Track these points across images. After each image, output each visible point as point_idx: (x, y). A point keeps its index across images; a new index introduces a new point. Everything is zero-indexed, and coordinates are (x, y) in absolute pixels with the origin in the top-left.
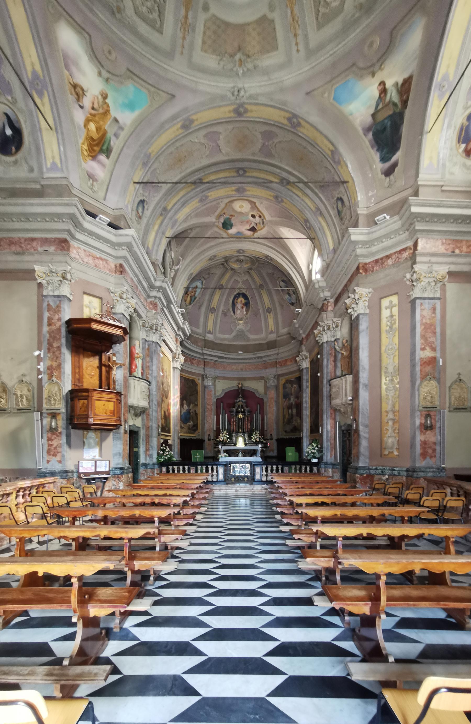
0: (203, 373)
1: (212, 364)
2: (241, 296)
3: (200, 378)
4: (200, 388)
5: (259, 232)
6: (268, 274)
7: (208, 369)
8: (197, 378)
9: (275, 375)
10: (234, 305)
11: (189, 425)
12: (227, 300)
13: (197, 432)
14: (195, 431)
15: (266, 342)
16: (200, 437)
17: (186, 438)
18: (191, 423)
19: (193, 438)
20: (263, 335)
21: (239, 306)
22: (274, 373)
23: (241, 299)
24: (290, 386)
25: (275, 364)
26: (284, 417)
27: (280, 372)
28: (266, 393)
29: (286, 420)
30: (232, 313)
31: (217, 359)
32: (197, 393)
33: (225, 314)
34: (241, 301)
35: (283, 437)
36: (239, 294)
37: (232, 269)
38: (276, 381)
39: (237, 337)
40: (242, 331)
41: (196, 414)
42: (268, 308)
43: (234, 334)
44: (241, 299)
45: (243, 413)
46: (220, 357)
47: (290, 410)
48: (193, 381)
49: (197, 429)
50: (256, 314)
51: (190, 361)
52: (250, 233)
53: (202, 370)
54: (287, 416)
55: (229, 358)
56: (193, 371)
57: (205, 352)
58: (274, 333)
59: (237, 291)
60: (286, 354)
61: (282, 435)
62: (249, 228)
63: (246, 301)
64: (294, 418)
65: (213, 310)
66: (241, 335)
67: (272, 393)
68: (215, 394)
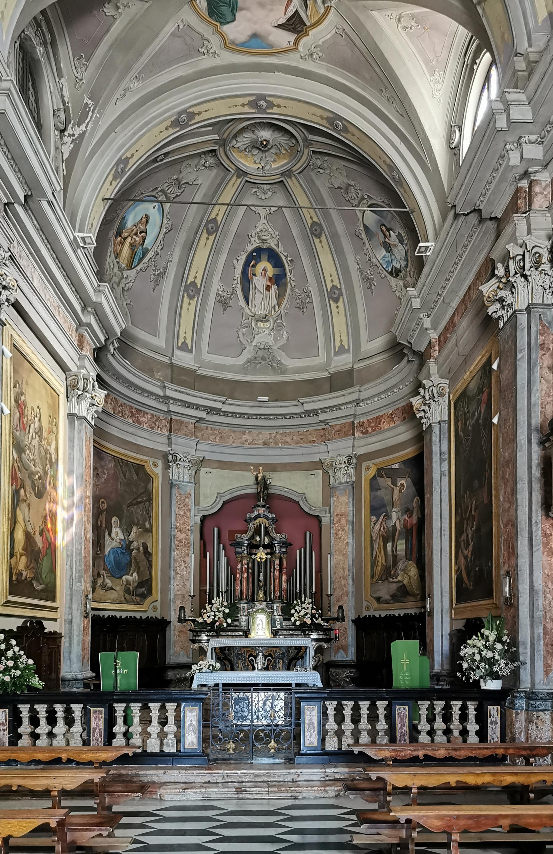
0: (165, 449)
1: (191, 427)
2: (264, 256)
3: (160, 463)
4: (158, 488)
5: (311, 33)
6: (334, 190)
7: (180, 440)
8: (151, 461)
9: (350, 457)
10: (246, 280)
11: (128, 583)
12: (229, 265)
13: (149, 600)
14: (144, 596)
15: (326, 374)
16: (158, 615)
17: (118, 615)
18: (133, 577)
19: (138, 615)
20: (321, 359)
21: (259, 282)
22: (349, 451)
23: (264, 264)
24: (389, 482)
25: (349, 429)
26: (373, 564)
27: (361, 451)
28: (326, 502)
29: (378, 569)
30: (242, 302)
31: (203, 414)
32: (150, 500)
33: (224, 303)
34: (265, 270)
35: (371, 613)
36: (258, 250)
37: (241, 173)
38: (352, 471)
39: (252, 364)
40: (267, 348)
41: (147, 554)
42: (334, 287)
43: (247, 355)
44: (264, 265)
45: (269, 546)
46: (211, 411)
47: (389, 545)
48: (140, 469)
49: (150, 592)
50: (303, 305)
51: (132, 415)
52: (285, 38)
53: (165, 440)
54: (381, 560)
55: (234, 415)
56: (140, 442)
57: (169, 393)
58: (348, 351)
59: (255, 244)
60: (377, 403)
61: (368, 608)
62: (282, 21)
63: (277, 271)
64: (400, 565)
65: (192, 290)
66: (264, 358)
67: (343, 503)
68: (197, 503)
